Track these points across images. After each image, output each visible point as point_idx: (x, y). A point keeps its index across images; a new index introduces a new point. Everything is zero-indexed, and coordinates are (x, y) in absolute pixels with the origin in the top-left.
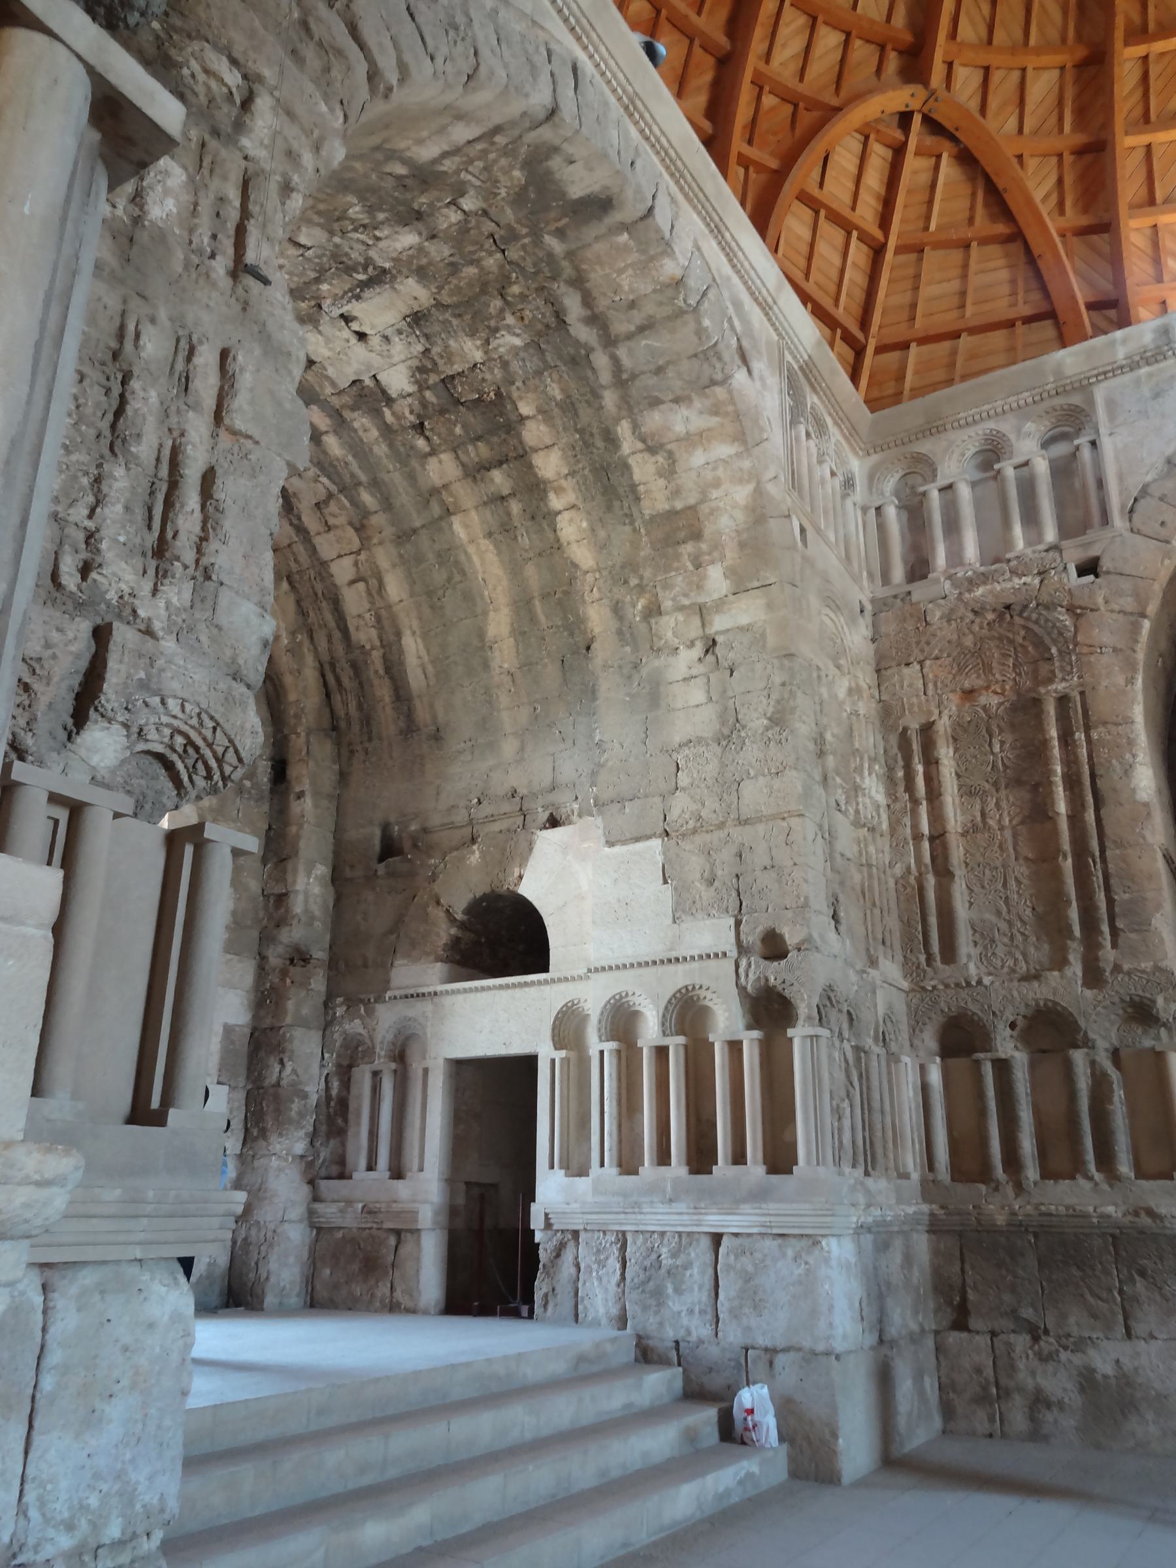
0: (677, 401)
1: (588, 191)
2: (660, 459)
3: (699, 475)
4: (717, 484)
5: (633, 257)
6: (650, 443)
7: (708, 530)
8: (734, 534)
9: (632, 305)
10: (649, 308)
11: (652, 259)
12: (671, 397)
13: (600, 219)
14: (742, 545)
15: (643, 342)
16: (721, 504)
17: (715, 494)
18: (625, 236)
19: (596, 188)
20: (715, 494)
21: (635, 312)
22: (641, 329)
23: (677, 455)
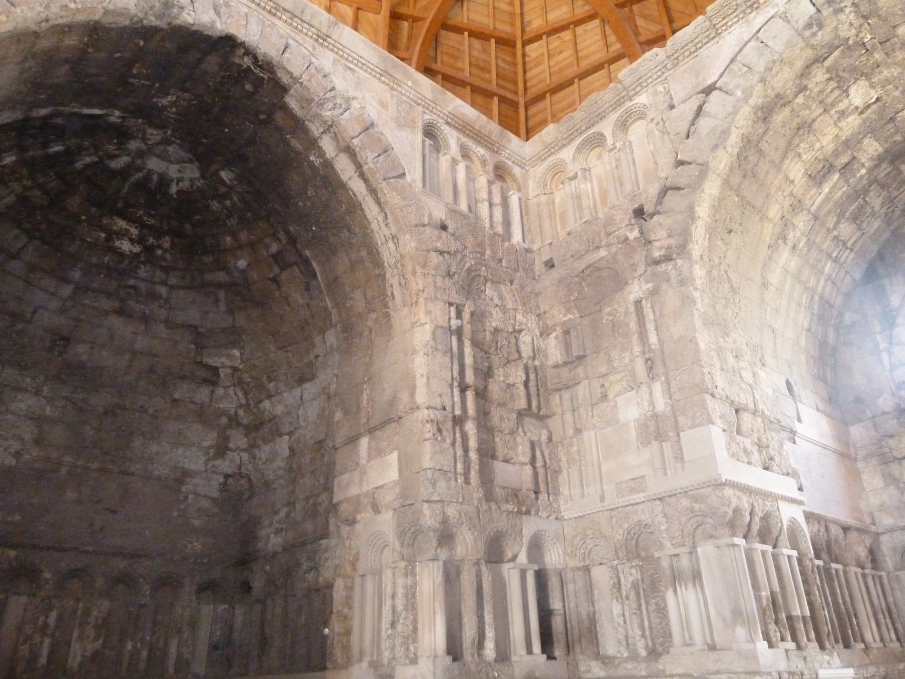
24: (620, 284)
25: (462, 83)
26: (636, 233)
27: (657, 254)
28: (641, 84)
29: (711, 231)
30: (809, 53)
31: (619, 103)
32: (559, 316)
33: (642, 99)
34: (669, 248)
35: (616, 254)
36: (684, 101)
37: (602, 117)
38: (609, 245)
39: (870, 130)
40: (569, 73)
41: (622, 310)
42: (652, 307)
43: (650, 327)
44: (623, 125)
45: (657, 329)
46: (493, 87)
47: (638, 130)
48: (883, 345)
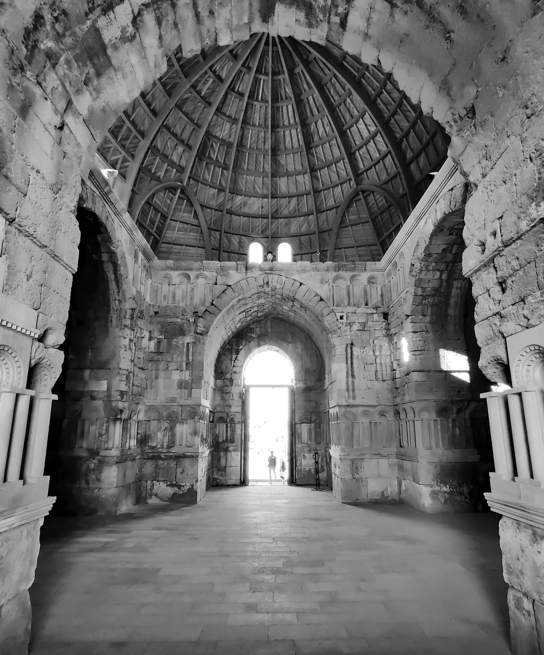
0: (160, 38)
1: (276, 14)
2: (131, 29)
3: (126, 62)
4: (124, 77)
5: (235, 22)
6: (138, 19)
7: (104, 80)
8: (106, 102)
9: (211, 13)
10: (207, 23)
11: (231, 32)
12: (163, 33)
13: (260, 11)
14: (104, 110)
15: (191, 15)
16: (116, 84)
17: (120, 76)
18: (246, 20)
19: (275, 19)
20: (120, 76)
21: (208, 14)
22: (197, 15)
23: (134, 43)
24: (182, 332)
25: (144, 228)
26: (193, 320)
27: (198, 331)
28: (209, 269)
29: (214, 328)
30: (257, 292)
31: (199, 269)
32: (156, 334)
33: (207, 273)
34: (203, 331)
35: (184, 323)
36: (221, 285)
37: (191, 269)
38: (182, 319)
39: (258, 306)
40: (182, 241)
41: (181, 342)
42: (193, 347)
43: (190, 354)
44: (197, 277)
45: (193, 355)
46: (153, 231)
47: (201, 281)
48: (234, 359)
